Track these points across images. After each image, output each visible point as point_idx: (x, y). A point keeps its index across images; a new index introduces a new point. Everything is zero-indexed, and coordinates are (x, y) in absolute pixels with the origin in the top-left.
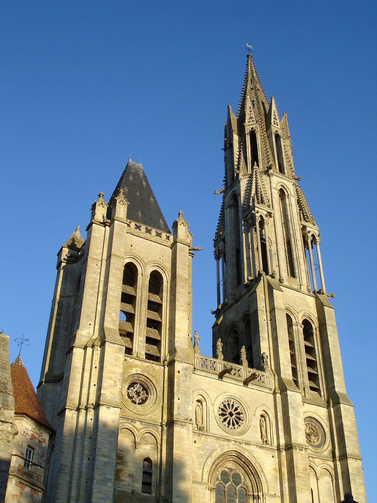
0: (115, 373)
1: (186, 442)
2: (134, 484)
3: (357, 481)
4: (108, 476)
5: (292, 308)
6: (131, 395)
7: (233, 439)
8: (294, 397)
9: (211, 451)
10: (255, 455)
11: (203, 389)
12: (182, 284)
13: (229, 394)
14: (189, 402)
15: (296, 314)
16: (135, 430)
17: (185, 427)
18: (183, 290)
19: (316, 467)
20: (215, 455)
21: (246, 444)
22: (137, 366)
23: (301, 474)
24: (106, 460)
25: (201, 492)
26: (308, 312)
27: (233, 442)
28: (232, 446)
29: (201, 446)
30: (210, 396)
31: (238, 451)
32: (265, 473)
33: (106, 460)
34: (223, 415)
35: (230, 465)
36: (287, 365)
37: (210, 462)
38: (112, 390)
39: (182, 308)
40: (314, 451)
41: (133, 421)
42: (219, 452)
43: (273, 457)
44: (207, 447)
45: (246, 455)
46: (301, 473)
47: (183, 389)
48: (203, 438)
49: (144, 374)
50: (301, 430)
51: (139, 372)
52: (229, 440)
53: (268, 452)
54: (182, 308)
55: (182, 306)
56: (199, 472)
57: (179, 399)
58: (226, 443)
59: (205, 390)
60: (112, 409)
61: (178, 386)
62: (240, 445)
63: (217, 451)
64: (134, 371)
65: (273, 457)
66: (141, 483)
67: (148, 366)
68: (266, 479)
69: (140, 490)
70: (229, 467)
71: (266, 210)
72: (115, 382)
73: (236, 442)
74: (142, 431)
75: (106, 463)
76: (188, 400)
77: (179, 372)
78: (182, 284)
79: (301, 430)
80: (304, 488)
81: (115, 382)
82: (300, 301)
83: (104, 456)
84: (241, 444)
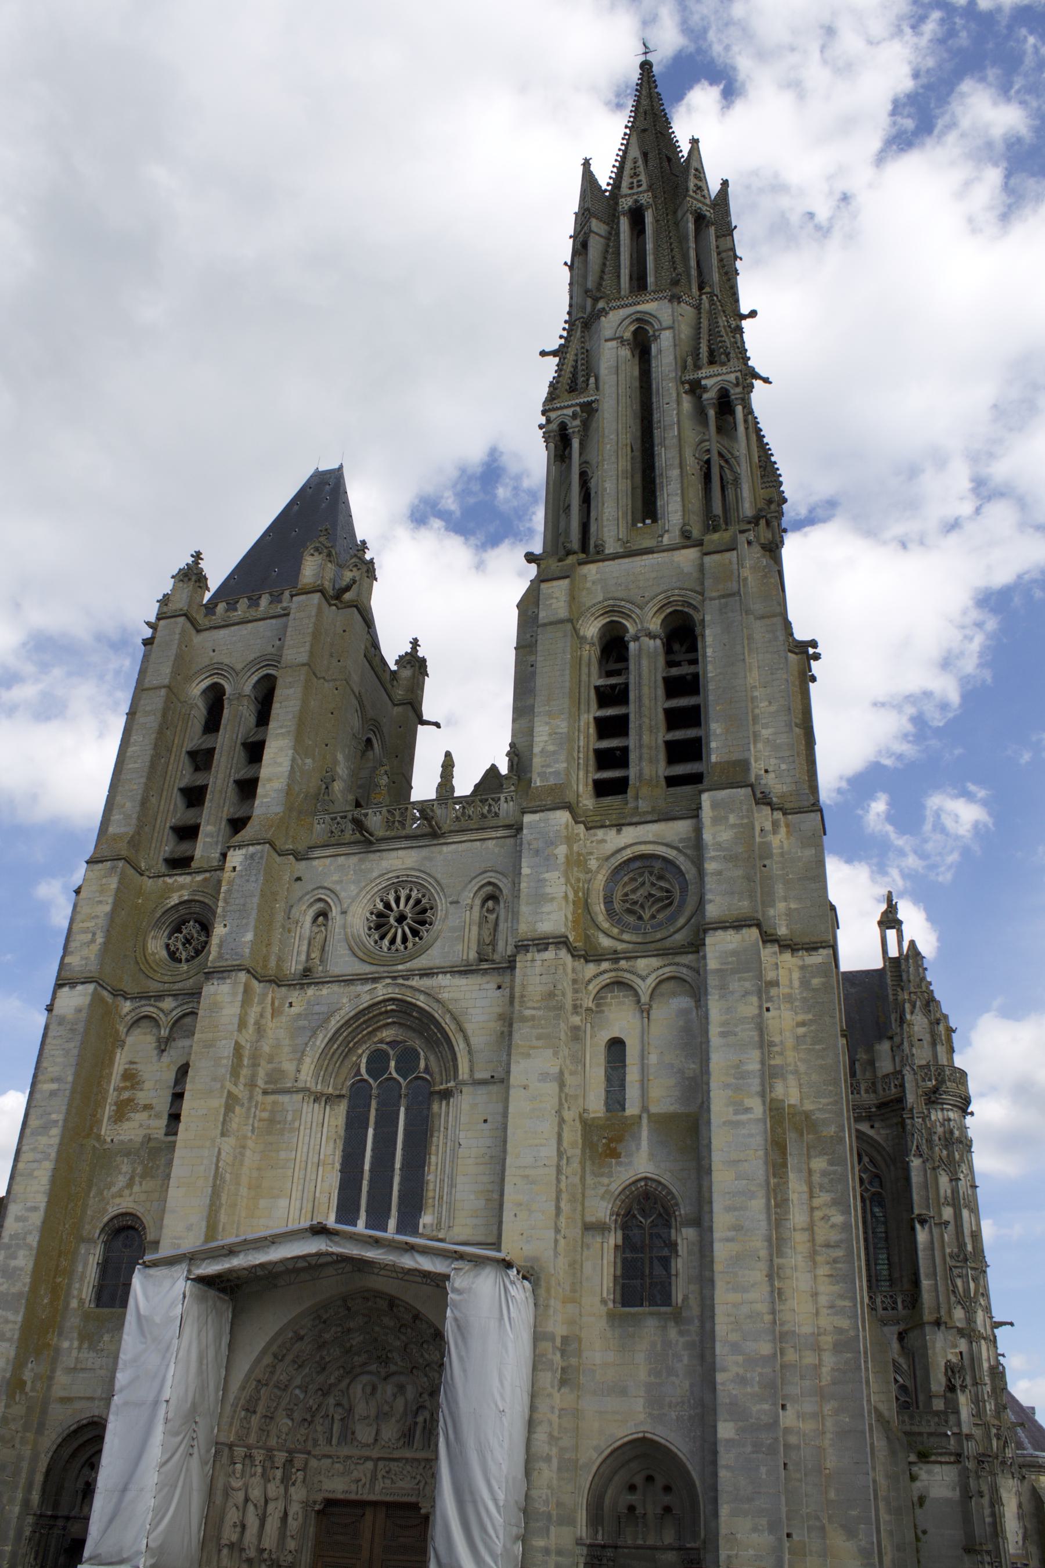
0: (97, 917)
1: (225, 1012)
2: (151, 1122)
3: (735, 985)
4: (54, 1117)
5: (623, 603)
6: (172, 948)
7: (386, 975)
8: (542, 825)
9: (321, 1017)
10: (445, 996)
11: (326, 885)
12: (290, 679)
13: (390, 875)
14: (247, 924)
15: (638, 611)
16: (161, 1015)
17: (228, 981)
18: (292, 691)
19: (639, 981)
20: (334, 1024)
21: (421, 976)
22: (182, 887)
23: (533, 1012)
24: (54, 1086)
25: (290, 1108)
26: (676, 592)
27: (389, 981)
28: (382, 991)
29: (305, 1009)
30: (343, 895)
31: (399, 996)
32: (469, 1032)
33: (54, 1086)
35: (388, 1034)
36: (554, 753)
37: (321, 1041)
38: (85, 952)
39: (283, 730)
40: (639, 940)
41: (160, 997)
43: (499, 987)
44: (317, 1009)
45: (421, 1001)
46: (534, 1008)
47: (237, 902)
48: (311, 991)
49: (197, 898)
50: (553, 899)
51: (186, 898)
52: (375, 980)
53: (487, 978)
54: (283, 730)
55: (281, 727)
57: (225, 926)
58: (368, 987)
59: (330, 886)
60: (80, 988)
61: (226, 901)
62: (406, 982)
63: (342, 1012)
64: (174, 900)
65: (499, 987)
66: (166, 1117)
67: (205, 880)
68: (468, 1044)
69: (163, 1131)
70: (388, 1040)
71: (574, 402)
72: (94, 934)
73: (394, 978)
74: (175, 1013)
75: (53, 1094)
76: (244, 921)
77: (234, 868)
78: (290, 679)
79: (553, 899)
80: (540, 1043)
81: (94, 934)
82: (654, 575)
83: (53, 1080)
84: (408, 979)
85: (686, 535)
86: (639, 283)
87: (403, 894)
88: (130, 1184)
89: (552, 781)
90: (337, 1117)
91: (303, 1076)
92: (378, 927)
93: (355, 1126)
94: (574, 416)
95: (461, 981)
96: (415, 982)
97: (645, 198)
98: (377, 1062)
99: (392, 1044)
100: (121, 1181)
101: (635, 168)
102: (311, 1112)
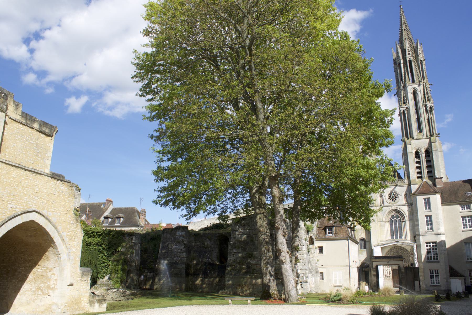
20: (387, 212)
28: (393, 208)
34: (390, 198)
35: (394, 213)
37: (385, 215)
42: (388, 210)
56: (382, 218)
85: (427, 136)
86: (413, 81)
87: (393, 193)
88: (362, 234)
89: (413, 179)
90: (389, 224)
91: (384, 219)
92: (390, 198)
93: (391, 225)
94: (405, 110)
95: (403, 206)
96: (397, 207)
97: (412, 58)
98: (393, 216)
99: (395, 214)
100: (360, 234)
101: (408, 49)
102: (386, 224)
